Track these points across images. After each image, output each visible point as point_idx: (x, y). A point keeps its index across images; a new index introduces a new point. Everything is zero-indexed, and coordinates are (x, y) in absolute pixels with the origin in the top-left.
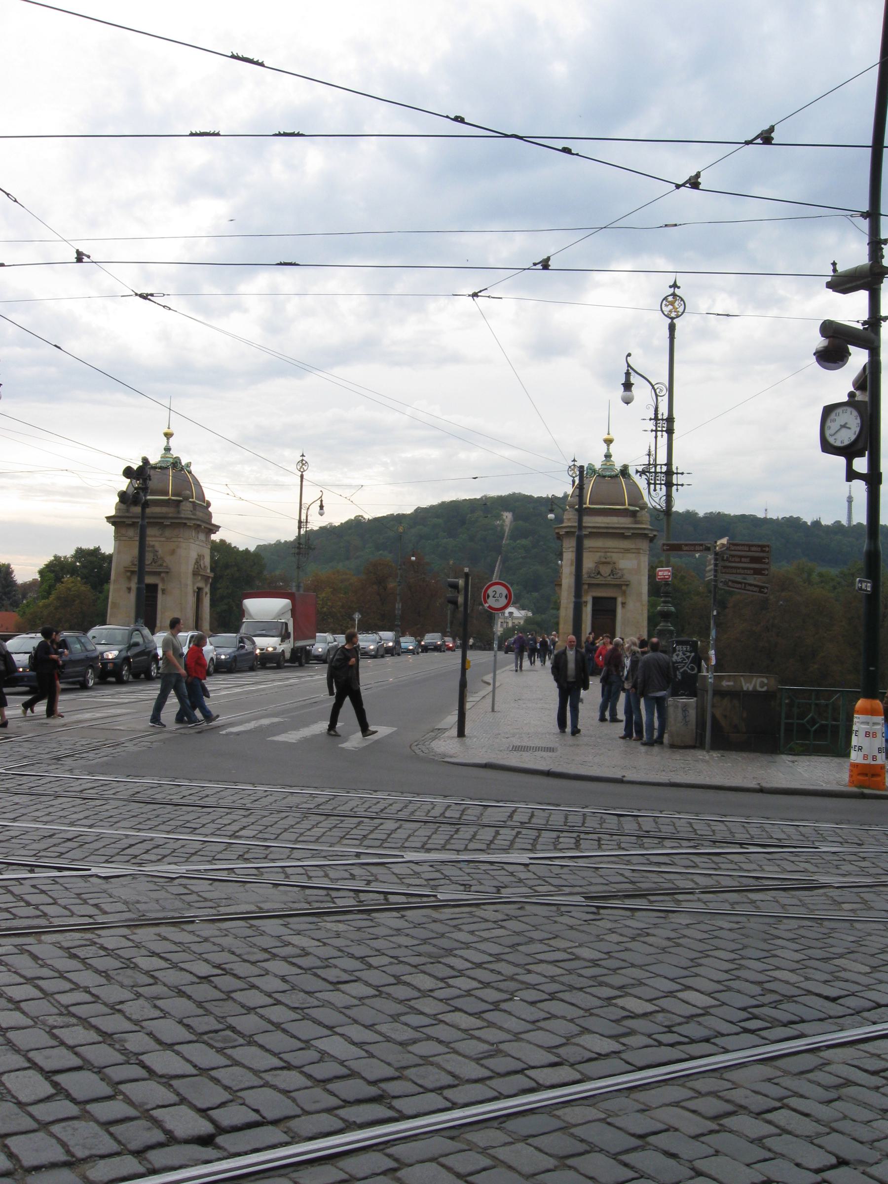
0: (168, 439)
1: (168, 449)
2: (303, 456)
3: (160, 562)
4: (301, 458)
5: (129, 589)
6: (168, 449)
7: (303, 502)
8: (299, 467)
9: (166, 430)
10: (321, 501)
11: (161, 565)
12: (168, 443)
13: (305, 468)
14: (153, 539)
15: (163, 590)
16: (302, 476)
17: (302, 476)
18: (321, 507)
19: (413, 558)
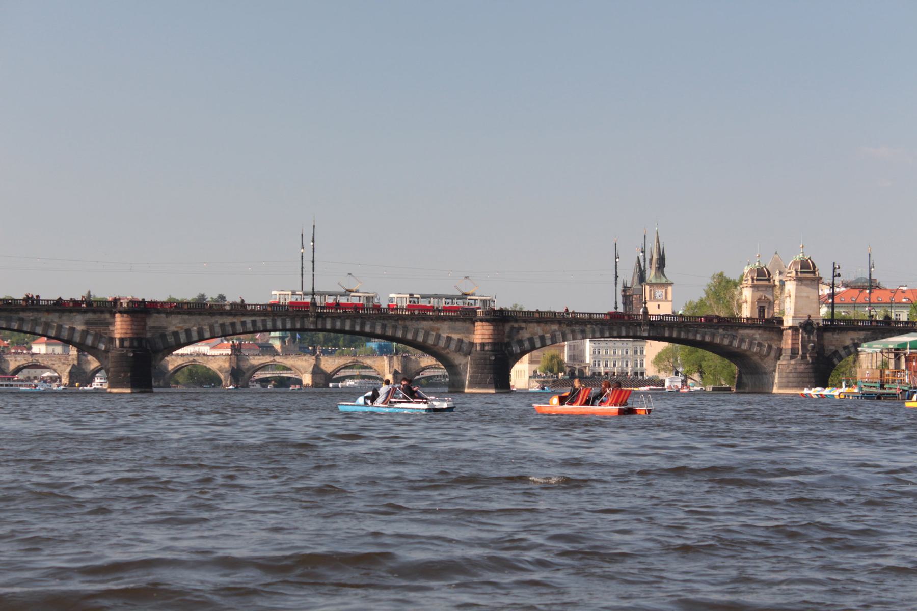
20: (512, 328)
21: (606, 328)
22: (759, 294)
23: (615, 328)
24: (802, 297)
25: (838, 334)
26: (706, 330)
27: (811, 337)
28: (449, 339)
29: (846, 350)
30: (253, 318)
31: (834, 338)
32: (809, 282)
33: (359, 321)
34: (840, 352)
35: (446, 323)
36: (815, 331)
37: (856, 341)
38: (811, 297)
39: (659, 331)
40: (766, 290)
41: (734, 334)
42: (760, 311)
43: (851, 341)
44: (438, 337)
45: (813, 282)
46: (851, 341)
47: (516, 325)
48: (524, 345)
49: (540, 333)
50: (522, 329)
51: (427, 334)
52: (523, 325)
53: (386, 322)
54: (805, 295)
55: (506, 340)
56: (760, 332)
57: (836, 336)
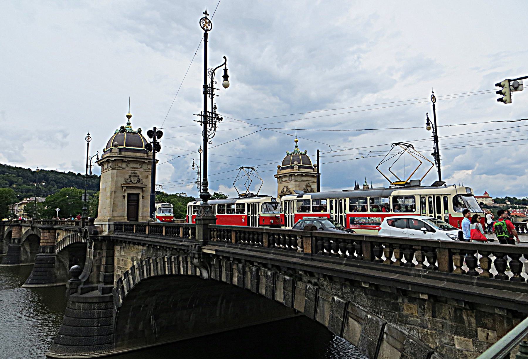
0: (129, 119)
2: (89, 134)
3: (141, 182)
4: (88, 135)
5: (124, 197)
6: (129, 124)
7: (89, 156)
8: (86, 140)
9: (128, 114)
10: (98, 156)
11: (142, 184)
12: (129, 120)
13: (90, 140)
14: (137, 170)
15: (143, 197)
19: (44, 184)
40: (289, 180)
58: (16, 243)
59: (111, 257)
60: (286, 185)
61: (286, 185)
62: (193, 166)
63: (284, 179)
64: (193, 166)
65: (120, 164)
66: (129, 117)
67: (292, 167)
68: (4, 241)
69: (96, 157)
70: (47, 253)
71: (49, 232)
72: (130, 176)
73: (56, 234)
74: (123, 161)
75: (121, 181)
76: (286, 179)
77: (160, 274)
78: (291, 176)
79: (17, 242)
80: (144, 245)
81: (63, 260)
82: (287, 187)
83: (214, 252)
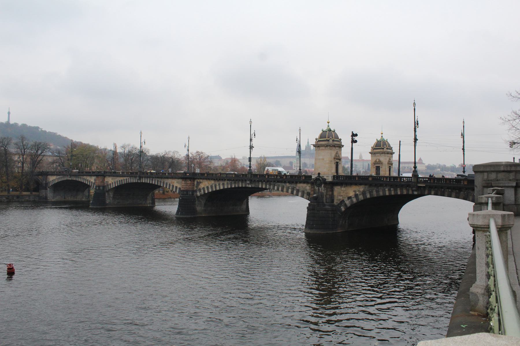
1: (328, 126)
6: (328, 126)
16: (251, 125)
17: (251, 125)
18: (255, 135)
20: (197, 182)
21: (233, 182)
22: (375, 158)
23: (237, 182)
24: (320, 159)
25: (344, 187)
26: (280, 184)
27: (320, 188)
28: (176, 187)
29: (349, 200)
30: (126, 178)
31: (342, 190)
32: (323, 148)
33: (151, 179)
34: (346, 202)
35: (176, 179)
36: (323, 185)
37: (357, 193)
38: (325, 159)
39: (256, 184)
41: (295, 186)
42: (377, 169)
43: (354, 193)
44: (173, 186)
45: (326, 148)
46: (354, 193)
47: (199, 181)
48: (201, 191)
49: (207, 185)
50: (200, 183)
51: (170, 185)
52: (201, 181)
53: (158, 179)
54: (321, 157)
55: (195, 188)
56: (309, 185)
57: (343, 189)
58: (101, 190)
59: (332, 191)
60: (378, 158)
61: (378, 158)
62: (297, 140)
63: (377, 155)
64: (297, 140)
65: (333, 148)
66: (328, 122)
67: (383, 149)
68: (48, 189)
69: (254, 134)
70: (190, 195)
71: (190, 181)
72: (336, 153)
73: (194, 182)
74: (334, 146)
75: (333, 155)
76: (379, 155)
77: (376, 196)
78: (382, 153)
79: (102, 189)
80: (366, 184)
81: (201, 200)
82: (379, 160)
83: (425, 185)
